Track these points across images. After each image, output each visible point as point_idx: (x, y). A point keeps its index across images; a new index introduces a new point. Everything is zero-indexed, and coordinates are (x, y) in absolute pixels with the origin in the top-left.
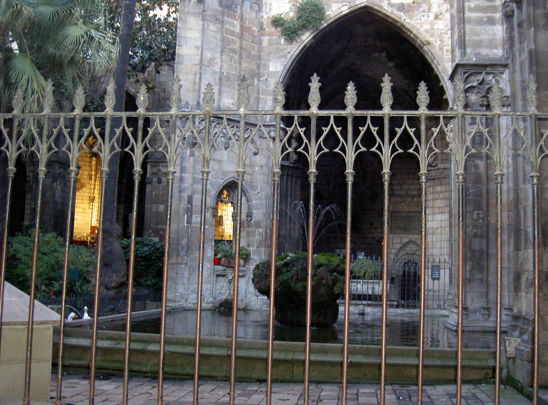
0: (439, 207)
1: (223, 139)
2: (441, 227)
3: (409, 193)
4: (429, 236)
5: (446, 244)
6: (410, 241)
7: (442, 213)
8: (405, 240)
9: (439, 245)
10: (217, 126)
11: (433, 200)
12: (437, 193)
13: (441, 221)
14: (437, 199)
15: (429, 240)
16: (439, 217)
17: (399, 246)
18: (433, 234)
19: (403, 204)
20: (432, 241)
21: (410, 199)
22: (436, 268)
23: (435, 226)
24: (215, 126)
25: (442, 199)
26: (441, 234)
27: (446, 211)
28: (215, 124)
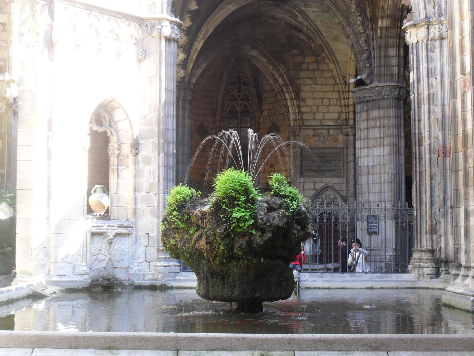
2: (380, 165)
3: (324, 123)
5: (386, 186)
8: (319, 186)
9: (377, 187)
12: (373, 119)
13: (380, 156)
14: (373, 128)
15: (363, 183)
16: (377, 151)
17: (312, 193)
18: (369, 174)
19: (317, 138)
20: (368, 184)
21: (324, 131)
22: (373, 220)
23: (371, 164)
27: (386, 143)
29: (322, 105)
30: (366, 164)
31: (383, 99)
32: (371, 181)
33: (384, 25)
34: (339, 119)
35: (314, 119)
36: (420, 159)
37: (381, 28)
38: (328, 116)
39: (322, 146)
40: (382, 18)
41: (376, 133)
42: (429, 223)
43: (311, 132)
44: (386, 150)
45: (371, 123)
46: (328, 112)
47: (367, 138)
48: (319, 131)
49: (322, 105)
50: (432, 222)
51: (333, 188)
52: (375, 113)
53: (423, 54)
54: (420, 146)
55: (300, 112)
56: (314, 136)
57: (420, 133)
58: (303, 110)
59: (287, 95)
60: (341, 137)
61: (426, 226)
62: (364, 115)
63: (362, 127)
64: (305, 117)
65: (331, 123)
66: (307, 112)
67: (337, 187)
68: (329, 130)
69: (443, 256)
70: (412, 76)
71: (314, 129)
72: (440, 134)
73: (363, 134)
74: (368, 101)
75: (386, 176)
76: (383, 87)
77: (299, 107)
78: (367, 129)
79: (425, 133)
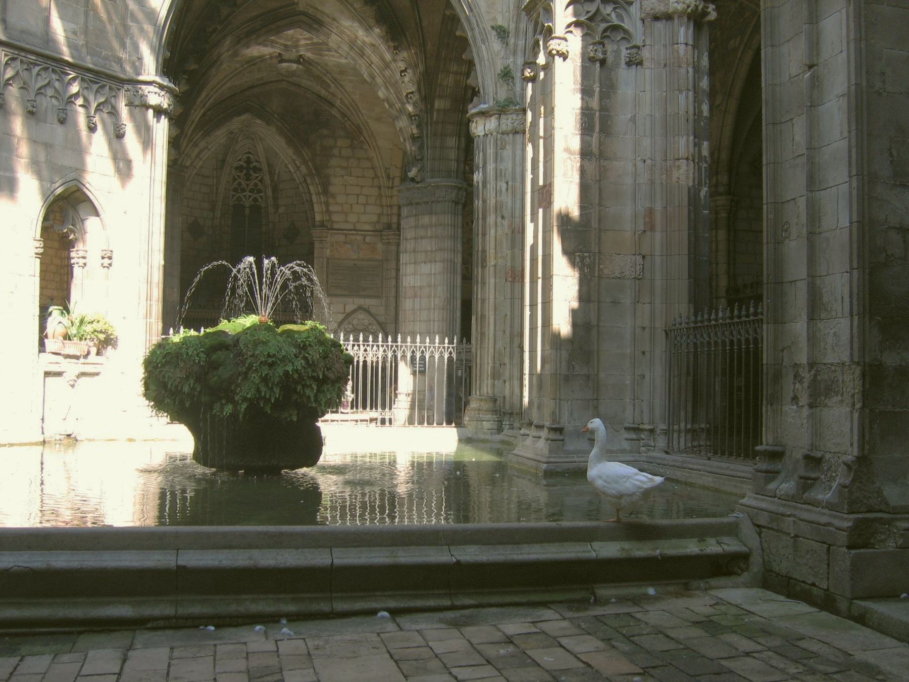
0: (426, 252)
1: (54, 101)
3: (358, 227)
4: (407, 301)
5: (436, 314)
6: (360, 308)
7: (430, 262)
8: (350, 308)
10: (43, 73)
11: (415, 238)
12: (423, 226)
13: (430, 274)
14: (422, 238)
15: (407, 308)
16: (425, 268)
18: (415, 296)
19: (349, 246)
20: (413, 309)
21: (358, 238)
24: (38, 74)
25: (431, 237)
26: (430, 297)
28: (37, 68)
29: (358, 203)
30: (412, 285)
31: (438, 202)
32: (417, 306)
33: (442, 107)
34: (378, 222)
35: (346, 221)
36: (484, 283)
37: (438, 110)
38: (364, 218)
39: (355, 257)
40: (440, 97)
41: (426, 245)
42: (491, 365)
43: (342, 238)
44: (437, 267)
45: (422, 232)
46: (365, 213)
47: (414, 251)
48: (353, 237)
49: (358, 203)
50: (494, 363)
51: (367, 311)
52: (425, 220)
53: (490, 151)
54: (484, 267)
55: (328, 211)
56: (345, 243)
57: (484, 251)
58: (332, 208)
59: (311, 188)
60: (380, 246)
61: (488, 368)
62: (412, 221)
63: (409, 237)
64: (335, 218)
65: (367, 227)
66: (337, 212)
67: (373, 311)
68: (365, 236)
69: (507, 407)
70: (477, 177)
71: (346, 235)
72: (509, 252)
73: (410, 245)
74: (417, 204)
75: (437, 301)
76: (438, 187)
77: (327, 204)
78: (415, 238)
79: (491, 253)
